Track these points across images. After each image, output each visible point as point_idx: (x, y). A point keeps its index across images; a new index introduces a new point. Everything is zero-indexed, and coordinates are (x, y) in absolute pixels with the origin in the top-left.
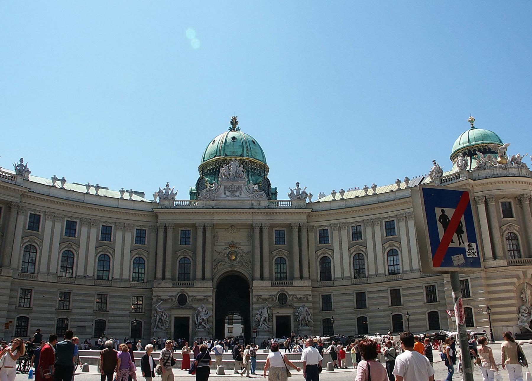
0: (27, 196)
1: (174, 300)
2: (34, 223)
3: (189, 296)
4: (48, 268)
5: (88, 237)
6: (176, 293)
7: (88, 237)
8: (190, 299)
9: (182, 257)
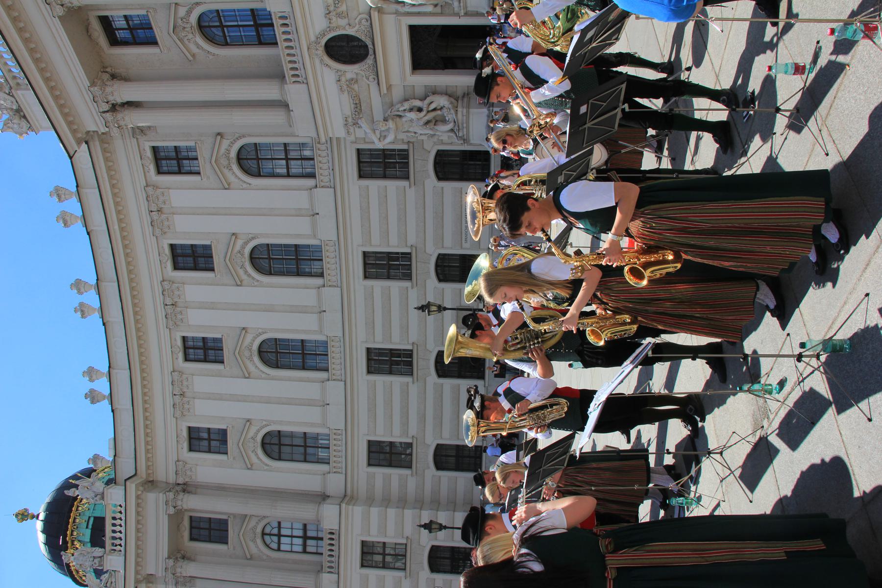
0: (148, 467)
1: (349, 76)
2: (209, 440)
3: (331, 29)
4: (310, 403)
5: (211, 306)
6: (326, 70)
7: (211, 306)
8: (343, 22)
9: (199, 40)
